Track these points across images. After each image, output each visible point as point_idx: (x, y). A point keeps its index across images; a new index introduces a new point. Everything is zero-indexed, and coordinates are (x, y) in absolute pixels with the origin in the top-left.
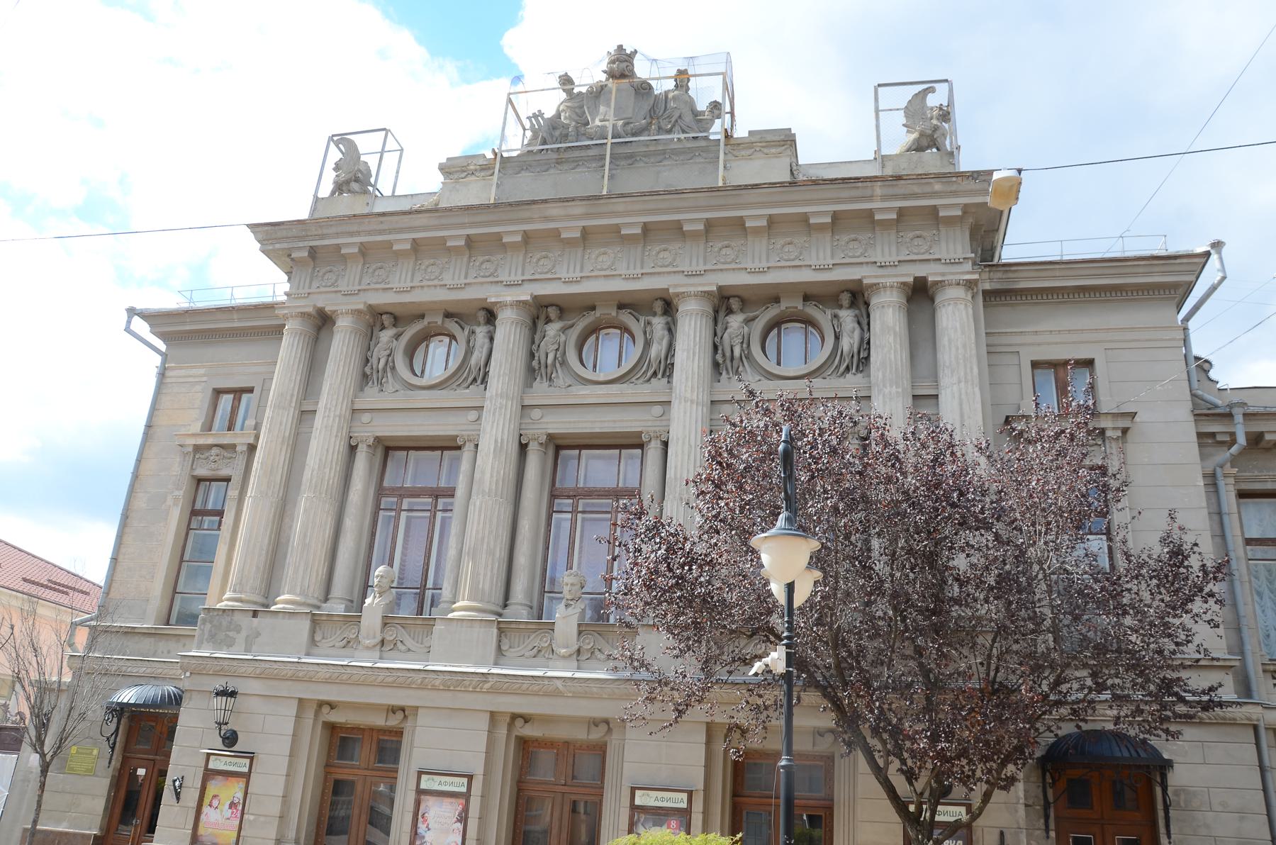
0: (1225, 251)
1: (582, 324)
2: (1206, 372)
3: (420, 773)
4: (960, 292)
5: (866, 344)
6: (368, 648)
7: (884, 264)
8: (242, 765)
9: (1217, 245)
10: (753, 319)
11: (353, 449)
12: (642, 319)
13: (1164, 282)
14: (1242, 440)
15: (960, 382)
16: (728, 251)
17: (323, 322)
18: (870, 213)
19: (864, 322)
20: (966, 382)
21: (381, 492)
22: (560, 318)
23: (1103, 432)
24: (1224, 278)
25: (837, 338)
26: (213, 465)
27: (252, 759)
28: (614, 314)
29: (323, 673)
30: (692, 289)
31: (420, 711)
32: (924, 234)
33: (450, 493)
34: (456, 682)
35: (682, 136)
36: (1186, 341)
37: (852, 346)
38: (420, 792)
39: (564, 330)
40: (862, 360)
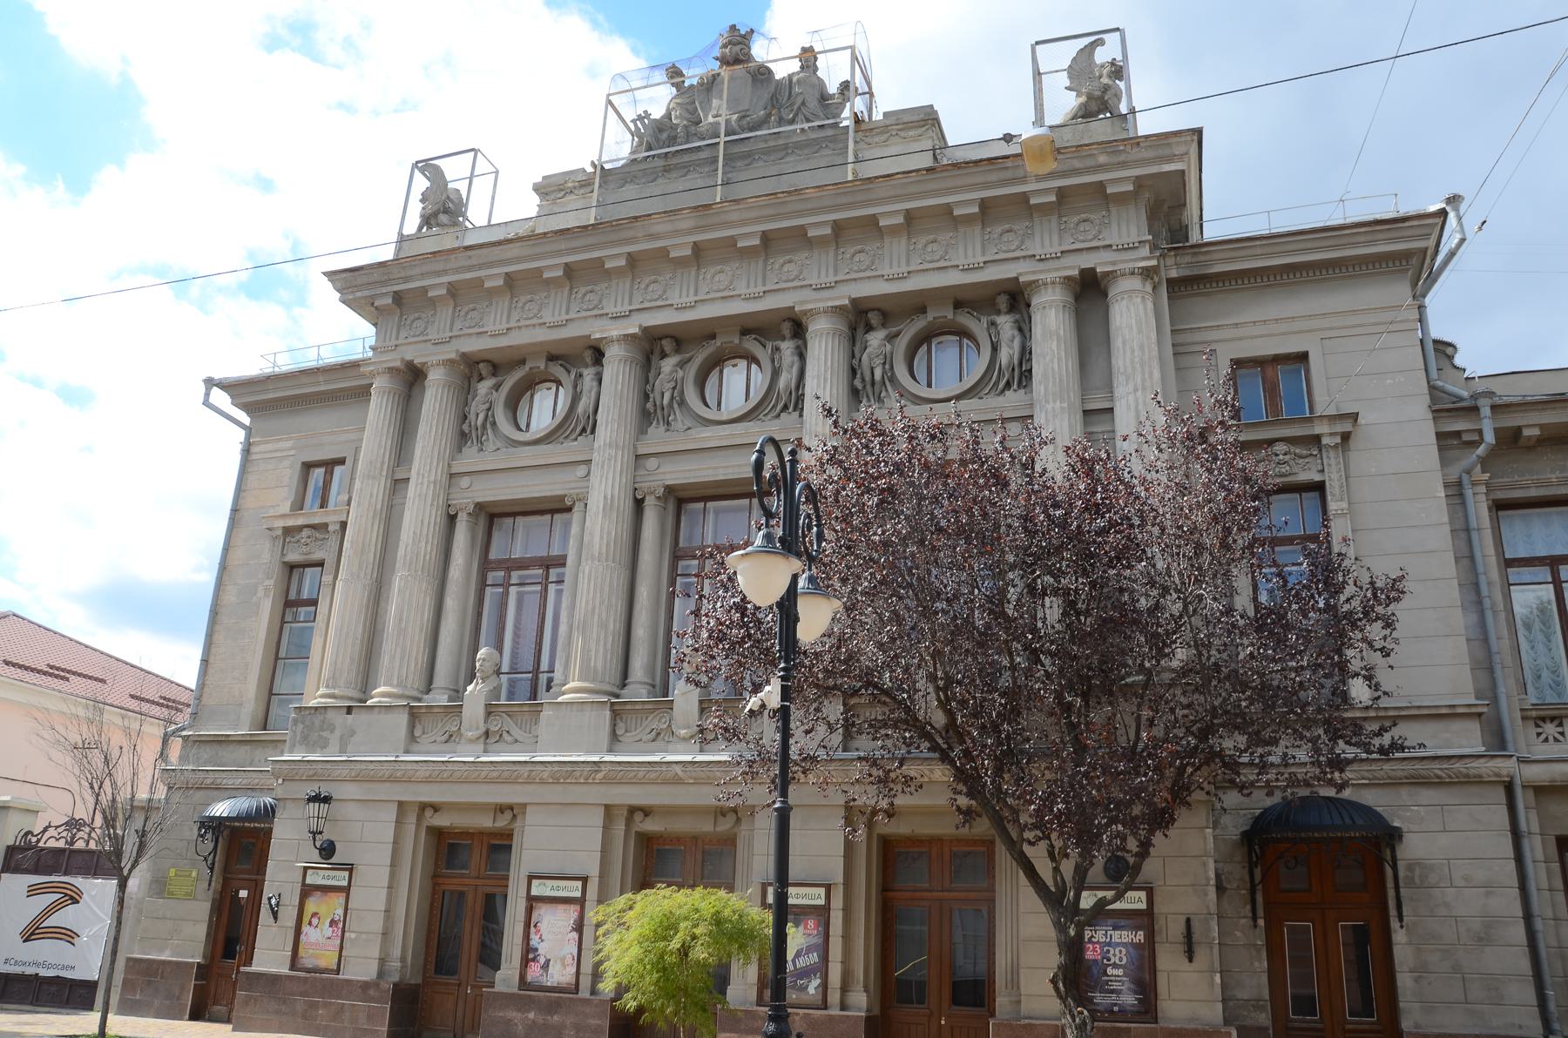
0: (1463, 207)
1: (700, 357)
2: (1451, 358)
3: (531, 878)
4: (1135, 283)
5: (1026, 353)
6: (471, 741)
7: (1043, 257)
8: (341, 879)
10: (897, 335)
11: (452, 519)
12: (769, 346)
13: (1403, 252)
14: (1489, 437)
15: (1136, 390)
16: (861, 256)
17: (412, 377)
19: (1026, 329)
20: (1144, 389)
21: (486, 565)
22: (678, 351)
23: (1316, 439)
24: (1463, 240)
25: (995, 349)
26: (304, 549)
27: (351, 871)
28: (737, 341)
29: (423, 772)
30: (821, 305)
32: (1092, 217)
33: (561, 562)
34: (565, 773)
35: (806, 126)
36: (1422, 320)
37: (1011, 358)
38: (532, 901)
39: (682, 365)
40: (1022, 375)
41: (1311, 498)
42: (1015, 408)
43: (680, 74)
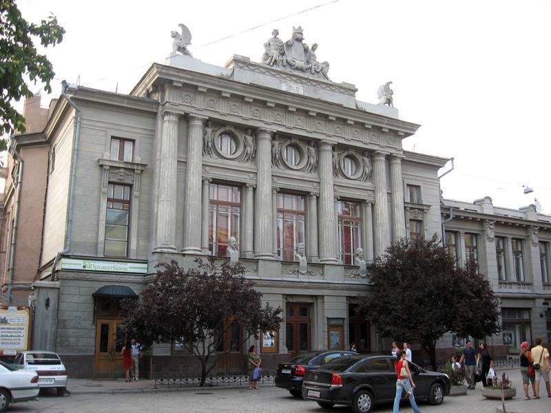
0: (454, 161)
9: (452, 159)
18: (381, 128)
24: (453, 169)
41: (127, 189)
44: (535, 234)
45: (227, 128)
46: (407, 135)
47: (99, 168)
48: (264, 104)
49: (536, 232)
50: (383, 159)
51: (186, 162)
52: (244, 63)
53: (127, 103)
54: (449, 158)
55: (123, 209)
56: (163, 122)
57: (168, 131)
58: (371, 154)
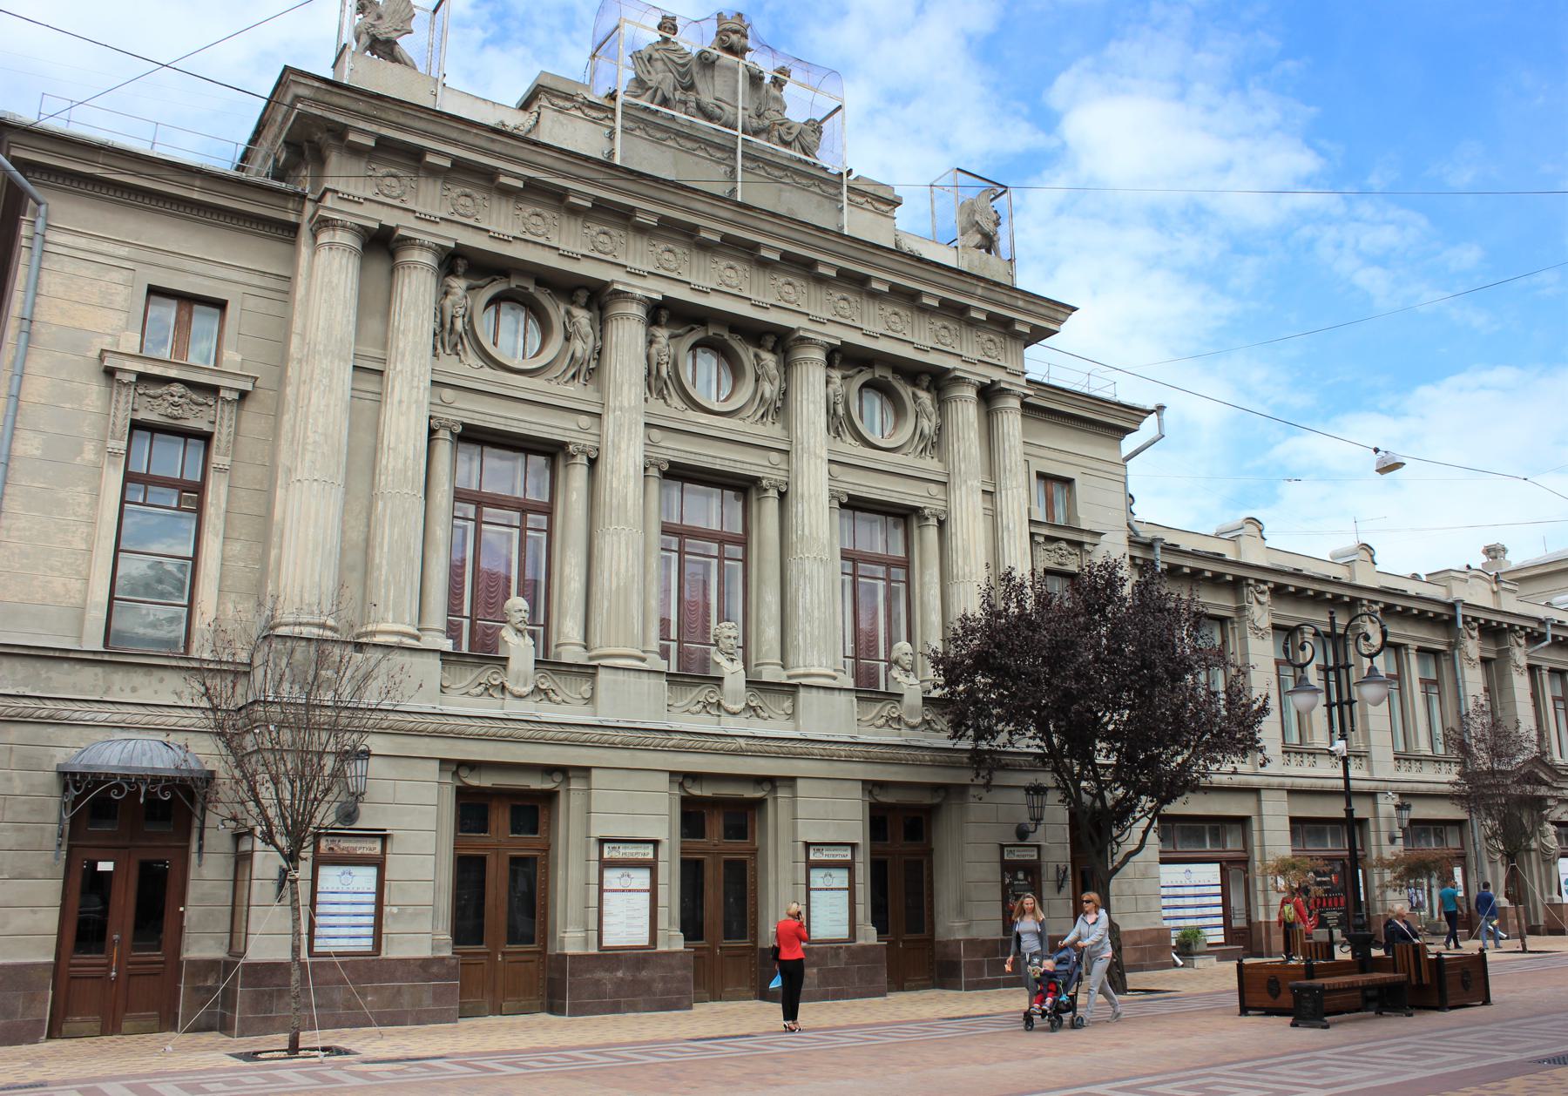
0: (1166, 414)
31: (594, 772)
34: (638, 738)
41: (196, 447)
42: (937, 473)
43: (674, 30)
44: (1259, 602)
45: (514, 283)
46: (1039, 334)
47: (102, 376)
48: (623, 217)
49: (1264, 598)
50: (971, 393)
51: (381, 373)
52: (568, 97)
53: (203, 190)
54: (1151, 407)
55: (178, 508)
56: (315, 247)
57: (329, 274)
58: (938, 381)
